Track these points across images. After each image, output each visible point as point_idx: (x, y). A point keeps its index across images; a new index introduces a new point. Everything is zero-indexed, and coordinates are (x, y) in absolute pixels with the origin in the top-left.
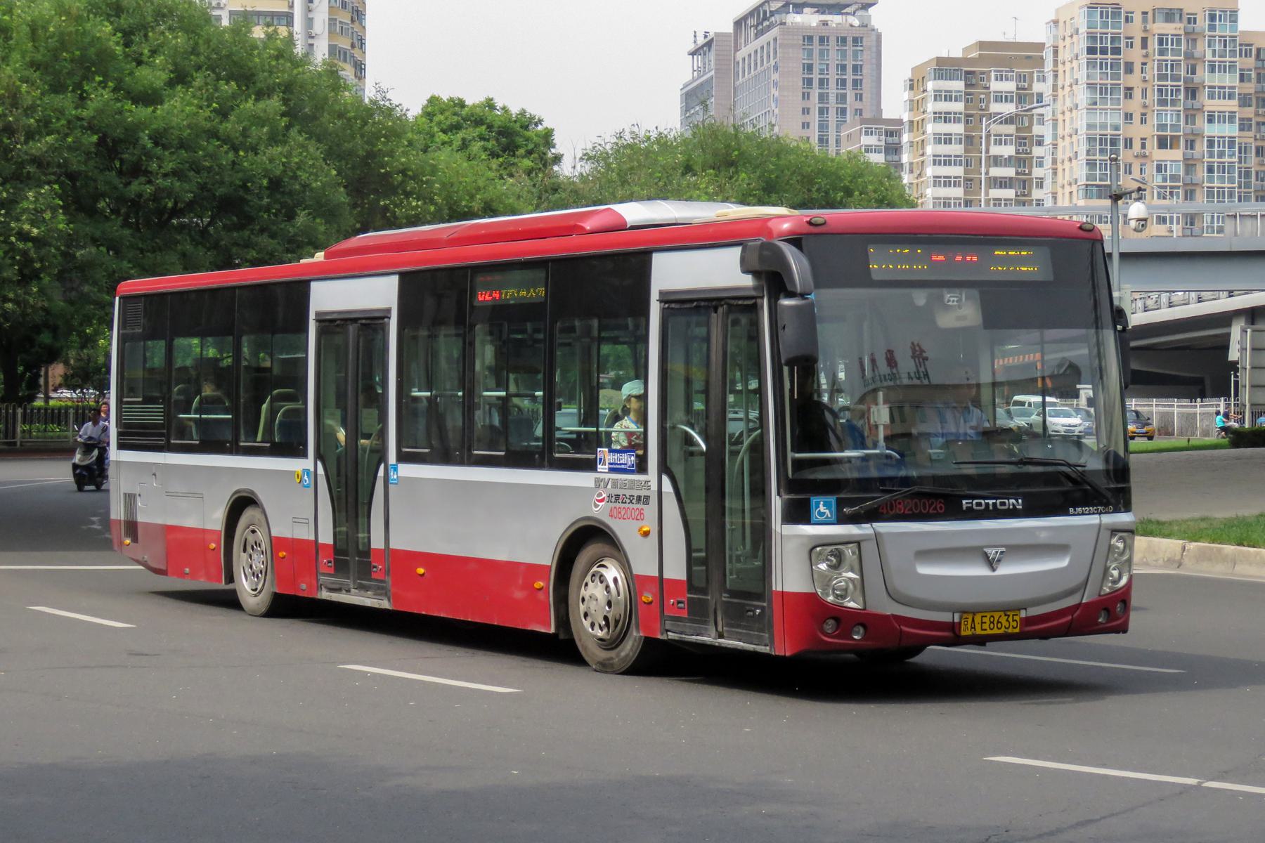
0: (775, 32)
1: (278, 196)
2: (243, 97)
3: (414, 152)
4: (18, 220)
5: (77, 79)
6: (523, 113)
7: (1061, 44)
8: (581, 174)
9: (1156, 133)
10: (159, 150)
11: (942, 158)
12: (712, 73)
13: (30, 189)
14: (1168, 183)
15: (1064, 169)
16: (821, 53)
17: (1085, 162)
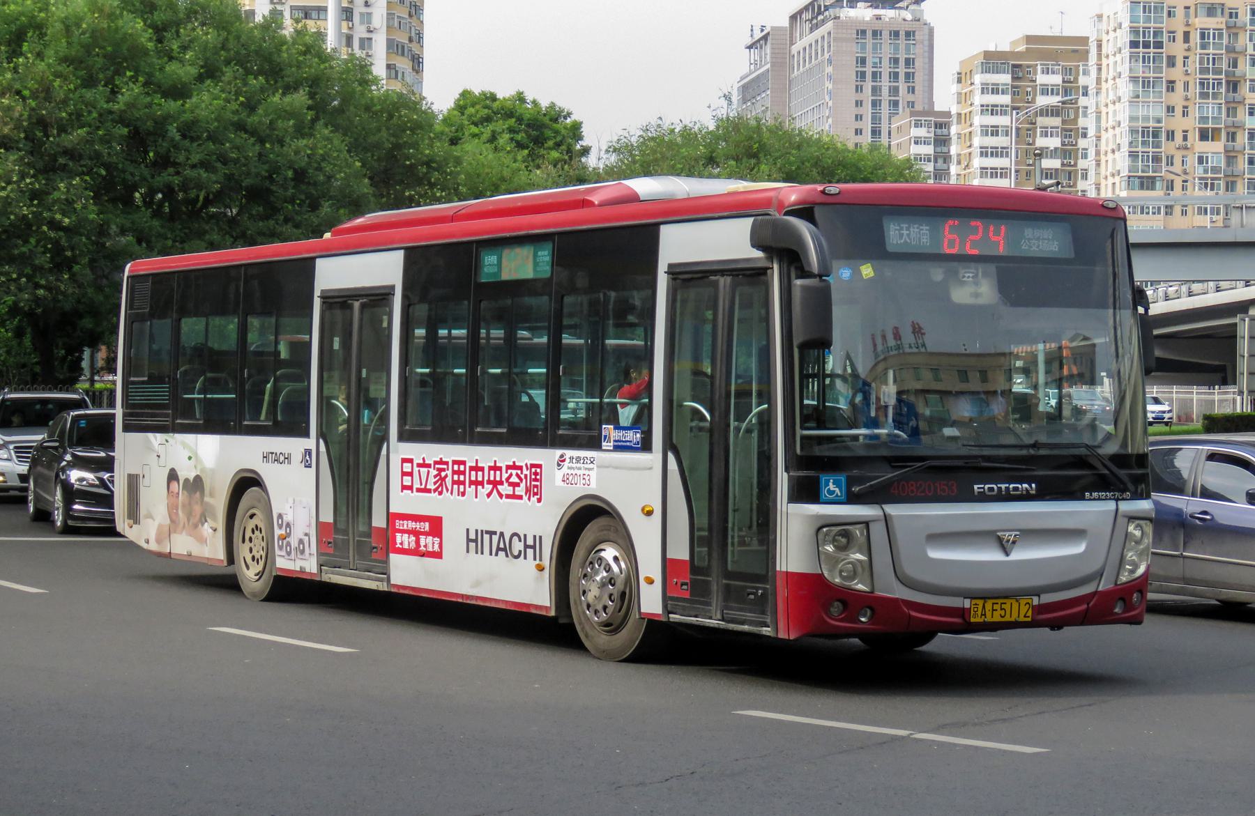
0: (829, 25)
1: (303, 187)
2: (270, 92)
3: (438, 144)
4: (50, 210)
5: (109, 73)
6: (553, 105)
7: (1105, 38)
8: (607, 166)
9: (1197, 125)
10: (187, 143)
11: (990, 150)
12: (768, 66)
13: (62, 180)
14: (1210, 175)
15: (1107, 161)
16: (875, 48)
17: (1127, 154)
